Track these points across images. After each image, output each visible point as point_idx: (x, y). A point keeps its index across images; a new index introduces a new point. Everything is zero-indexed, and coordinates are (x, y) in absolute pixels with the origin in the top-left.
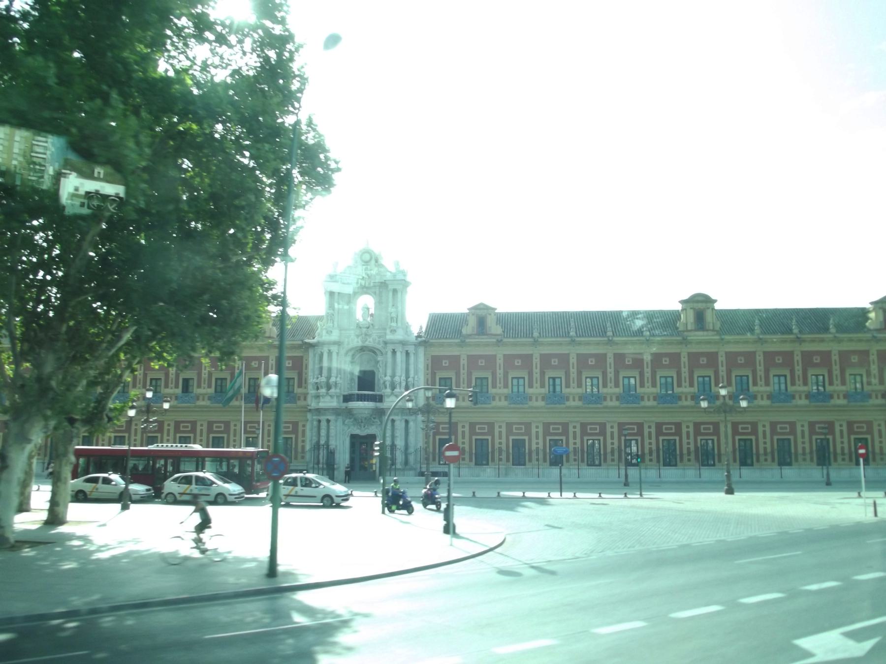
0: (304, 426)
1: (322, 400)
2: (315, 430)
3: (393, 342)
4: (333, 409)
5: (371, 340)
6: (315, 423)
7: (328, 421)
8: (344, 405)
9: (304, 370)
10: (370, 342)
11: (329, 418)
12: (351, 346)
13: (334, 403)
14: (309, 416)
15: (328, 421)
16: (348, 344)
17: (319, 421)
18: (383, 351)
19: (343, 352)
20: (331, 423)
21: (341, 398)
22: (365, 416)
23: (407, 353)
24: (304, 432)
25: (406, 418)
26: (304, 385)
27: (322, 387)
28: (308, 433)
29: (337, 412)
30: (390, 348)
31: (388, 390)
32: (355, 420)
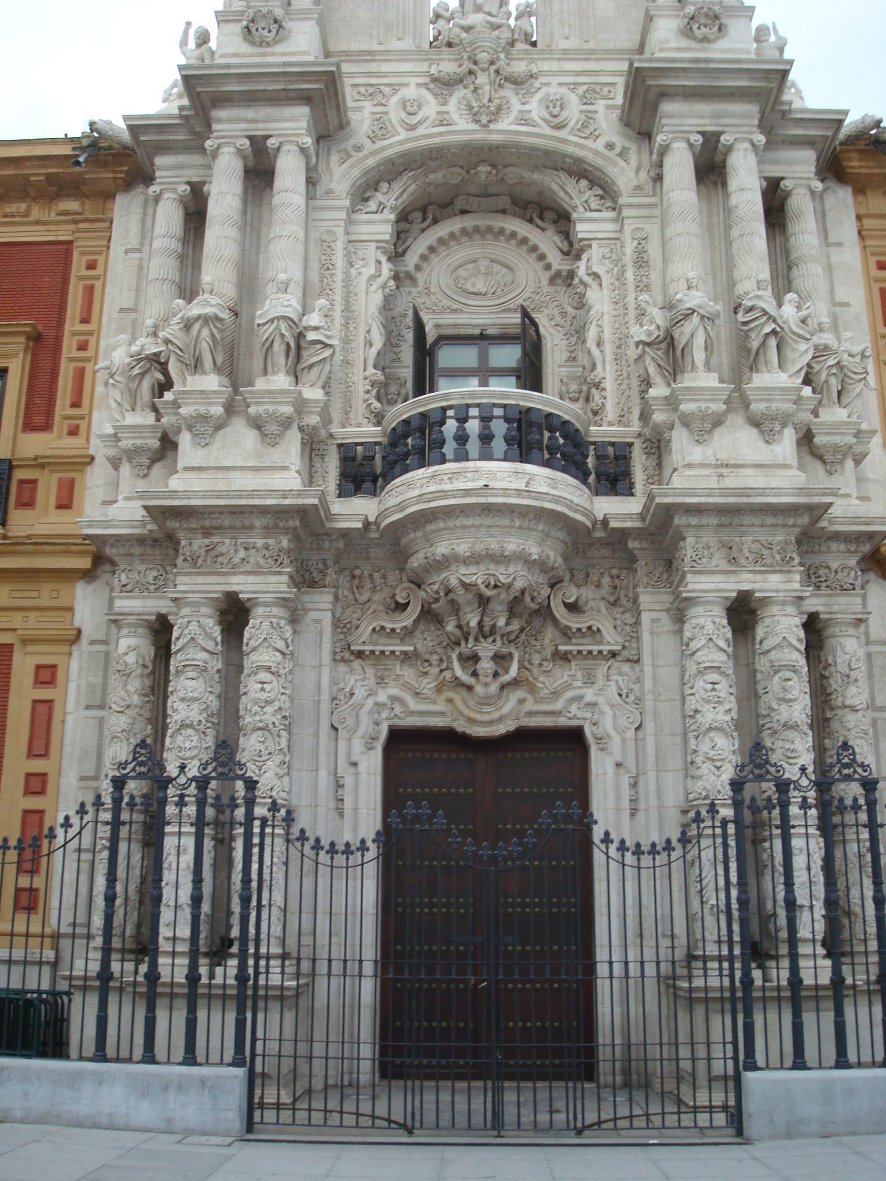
0: (46, 675)
1: (188, 451)
2: (129, 692)
3: (709, 87)
4: (277, 516)
5: (535, 108)
6: (132, 647)
7: (234, 614)
8: (354, 511)
9: (72, 324)
10: (521, 120)
11: (244, 585)
12: (399, 141)
13: (281, 476)
14: (87, 605)
15: (234, 614)
16: (381, 128)
17: (161, 631)
18: (625, 175)
19: (341, 177)
20: (257, 629)
21: (332, 465)
22: (519, 577)
23: (776, 207)
24: (43, 716)
25: (814, 604)
26: (63, 406)
27: (196, 366)
28: (74, 727)
29: (309, 544)
30: (681, 125)
31: (704, 379)
32: (429, 615)
